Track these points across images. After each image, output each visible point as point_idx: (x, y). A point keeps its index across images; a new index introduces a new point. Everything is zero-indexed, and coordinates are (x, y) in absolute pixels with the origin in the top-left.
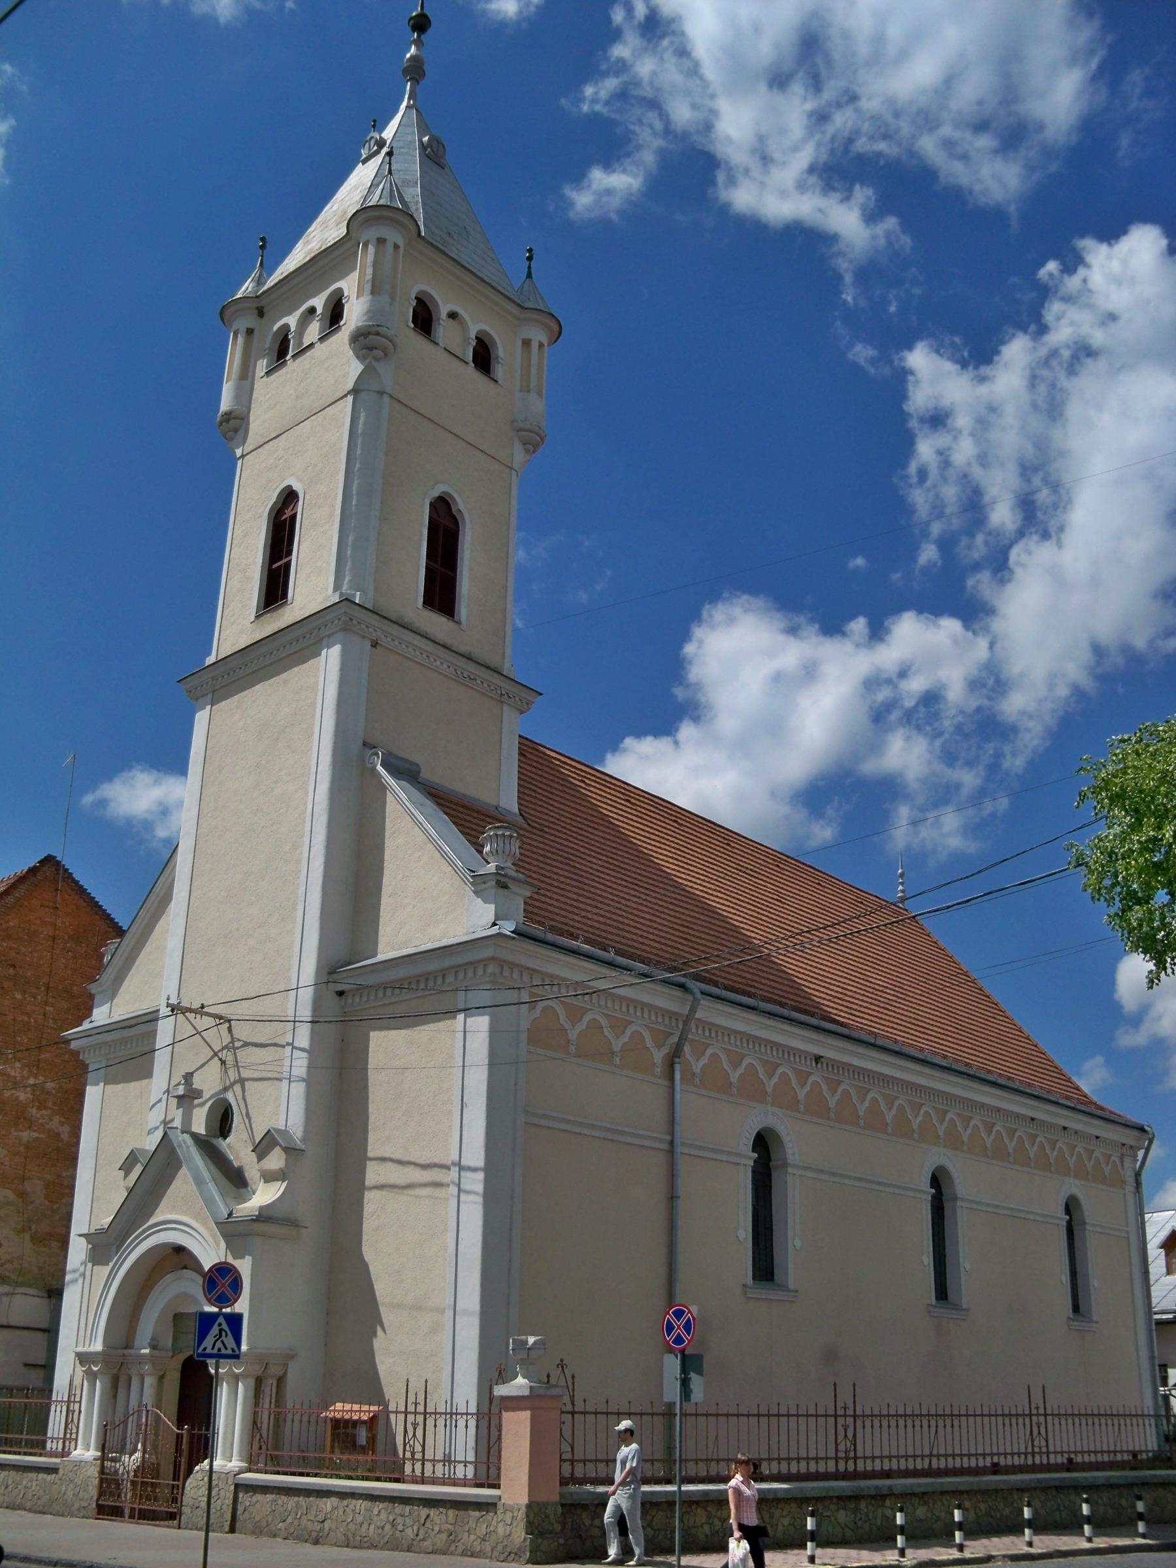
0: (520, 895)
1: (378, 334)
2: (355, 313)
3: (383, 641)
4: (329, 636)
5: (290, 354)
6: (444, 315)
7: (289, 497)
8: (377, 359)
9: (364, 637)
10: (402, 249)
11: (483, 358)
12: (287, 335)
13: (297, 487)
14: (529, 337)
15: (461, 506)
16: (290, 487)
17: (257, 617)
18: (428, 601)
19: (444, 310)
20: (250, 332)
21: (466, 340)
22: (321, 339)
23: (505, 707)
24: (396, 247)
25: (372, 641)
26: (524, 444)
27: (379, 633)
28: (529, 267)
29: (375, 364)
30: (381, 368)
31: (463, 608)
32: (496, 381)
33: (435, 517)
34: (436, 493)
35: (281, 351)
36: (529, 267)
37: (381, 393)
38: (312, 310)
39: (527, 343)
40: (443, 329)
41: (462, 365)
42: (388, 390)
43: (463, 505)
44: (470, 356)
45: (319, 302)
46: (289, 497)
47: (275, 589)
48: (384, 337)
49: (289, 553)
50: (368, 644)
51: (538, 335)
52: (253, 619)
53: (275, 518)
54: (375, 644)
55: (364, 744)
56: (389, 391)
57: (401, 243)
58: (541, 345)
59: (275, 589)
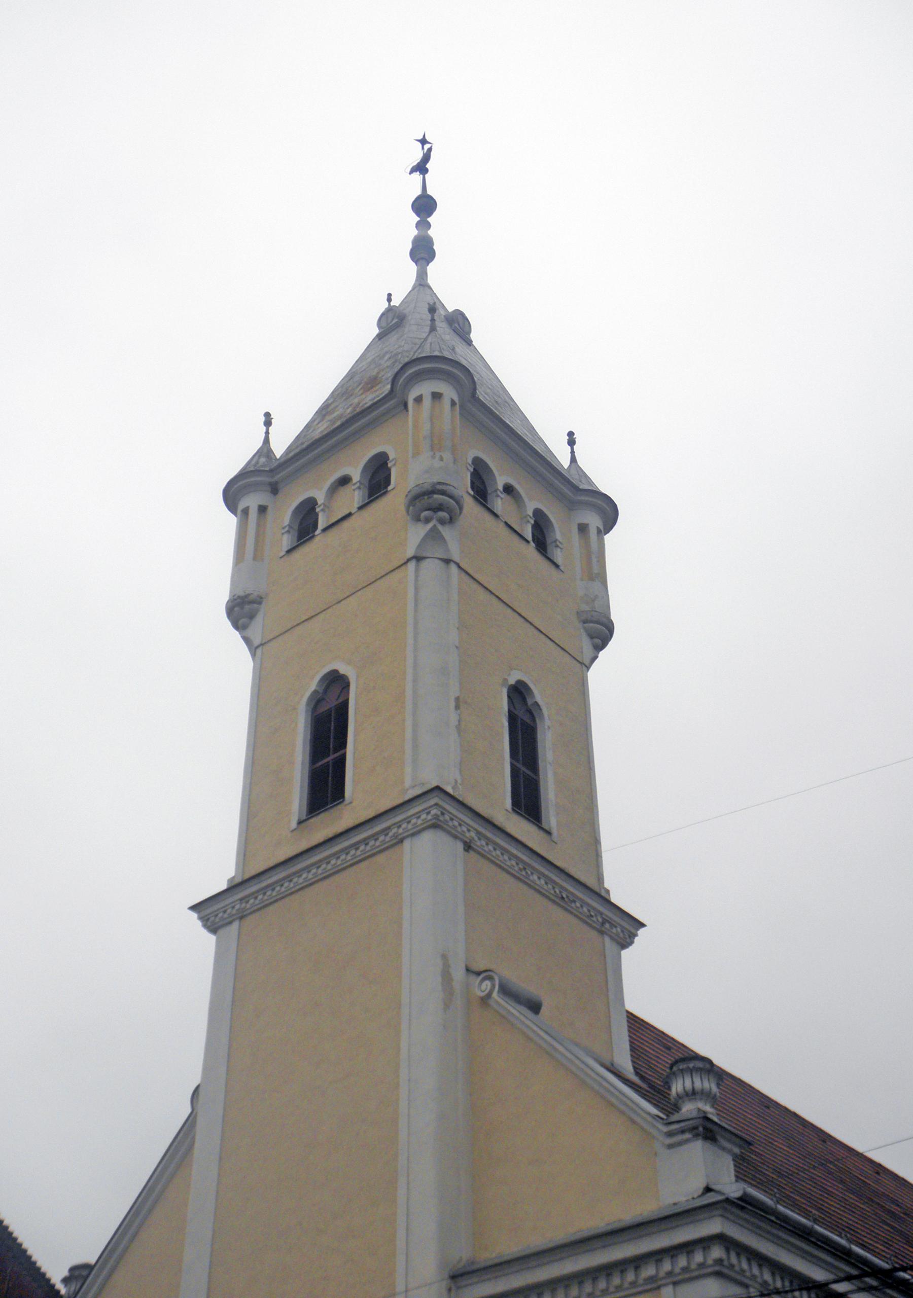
0: (729, 1151)
1: (443, 493)
2: (406, 478)
3: (479, 843)
4: (413, 835)
5: (321, 525)
6: (501, 488)
7: (336, 682)
8: (442, 522)
9: (456, 837)
10: (458, 406)
11: (541, 539)
12: (313, 509)
13: (343, 669)
14: (586, 521)
15: (538, 698)
16: (335, 672)
17: (300, 822)
18: (516, 804)
19: (501, 481)
20: (262, 509)
21: (524, 518)
22: (360, 508)
23: (607, 940)
24: (453, 403)
25: (465, 843)
26: (592, 637)
27: (473, 834)
28: (573, 452)
29: (440, 527)
30: (446, 532)
31: (551, 817)
32: (557, 566)
33: (512, 709)
34: (512, 681)
35: (306, 525)
36: (573, 452)
37: (447, 561)
38: (344, 481)
39: (583, 529)
40: (500, 503)
41: (524, 543)
42: (456, 557)
43: (539, 695)
44: (530, 538)
45: (354, 467)
46: (336, 682)
47: (326, 785)
48: (451, 497)
49: (343, 744)
50: (460, 846)
51: (594, 521)
52: (294, 824)
53: (315, 709)
54: (468, 847)
55: (468, 970)
56: (457, 559)
57: (456, 399)
58: (599, 532)
59: (326, 785)
